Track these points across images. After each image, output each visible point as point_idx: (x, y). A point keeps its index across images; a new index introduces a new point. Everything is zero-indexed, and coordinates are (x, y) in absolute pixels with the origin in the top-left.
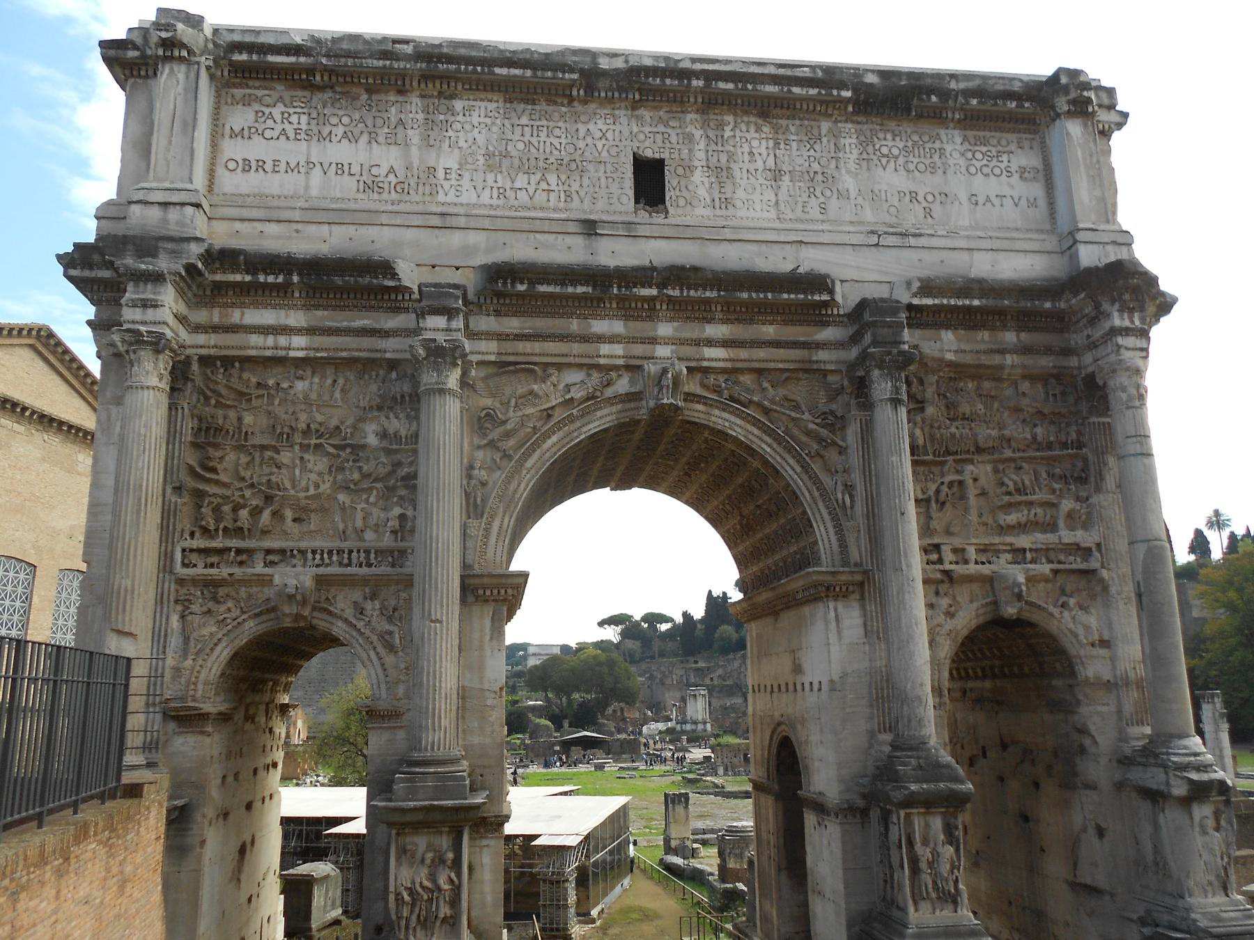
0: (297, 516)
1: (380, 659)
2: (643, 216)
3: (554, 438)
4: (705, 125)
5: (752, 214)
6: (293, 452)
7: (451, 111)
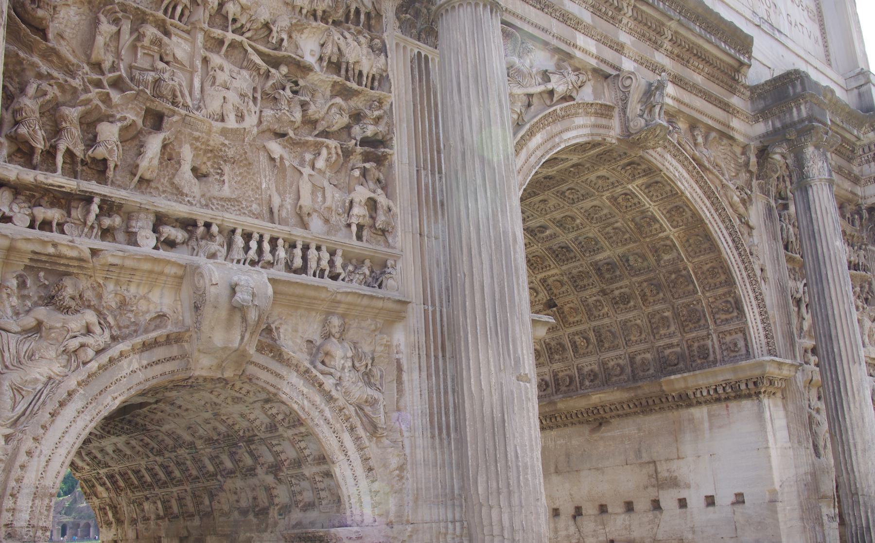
0: (197, 163)
1: (360, 448)
3: (538, 139)
6: (193, 43)
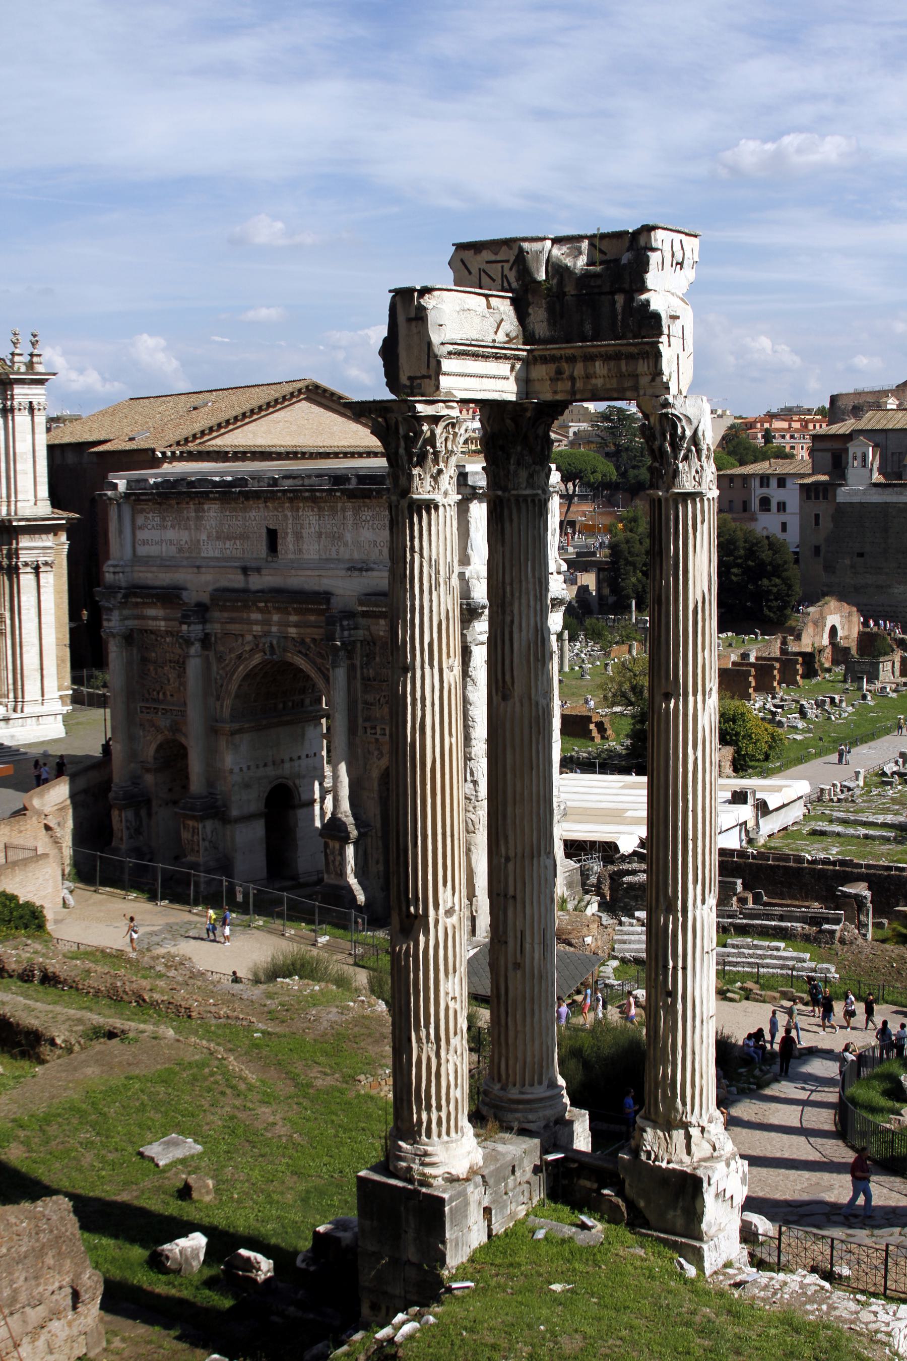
2: (270, 559)
3: (241, 667)
4: (292, 509)
5: (310, 557)
7: (203, 511)
